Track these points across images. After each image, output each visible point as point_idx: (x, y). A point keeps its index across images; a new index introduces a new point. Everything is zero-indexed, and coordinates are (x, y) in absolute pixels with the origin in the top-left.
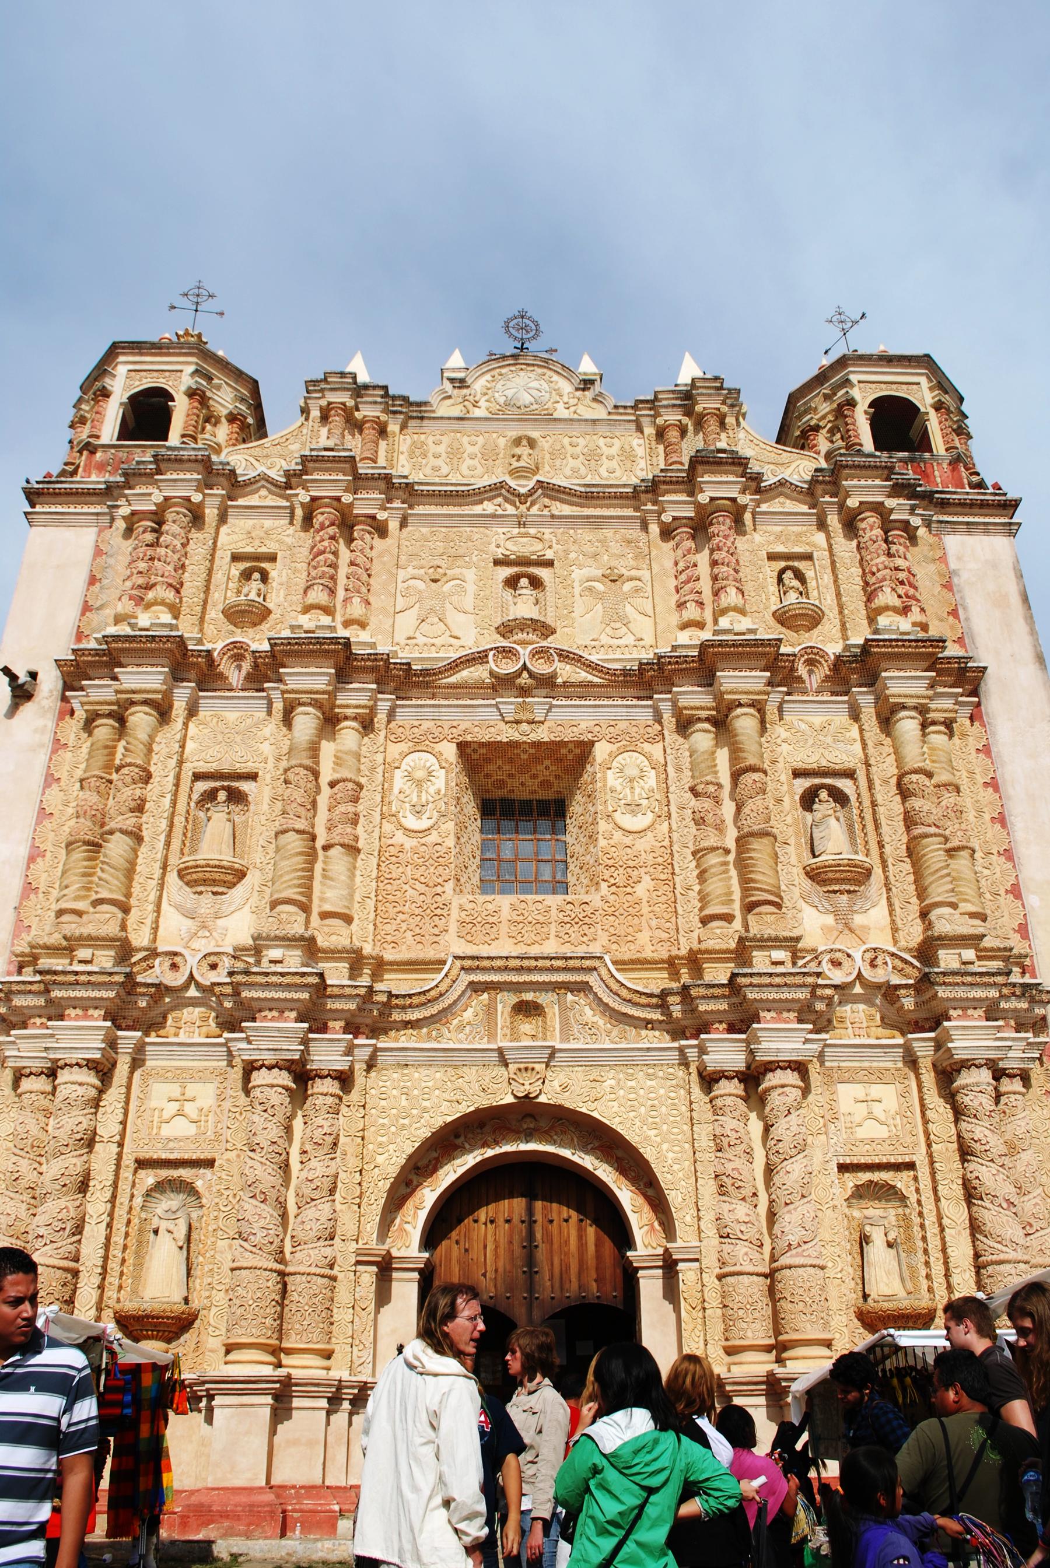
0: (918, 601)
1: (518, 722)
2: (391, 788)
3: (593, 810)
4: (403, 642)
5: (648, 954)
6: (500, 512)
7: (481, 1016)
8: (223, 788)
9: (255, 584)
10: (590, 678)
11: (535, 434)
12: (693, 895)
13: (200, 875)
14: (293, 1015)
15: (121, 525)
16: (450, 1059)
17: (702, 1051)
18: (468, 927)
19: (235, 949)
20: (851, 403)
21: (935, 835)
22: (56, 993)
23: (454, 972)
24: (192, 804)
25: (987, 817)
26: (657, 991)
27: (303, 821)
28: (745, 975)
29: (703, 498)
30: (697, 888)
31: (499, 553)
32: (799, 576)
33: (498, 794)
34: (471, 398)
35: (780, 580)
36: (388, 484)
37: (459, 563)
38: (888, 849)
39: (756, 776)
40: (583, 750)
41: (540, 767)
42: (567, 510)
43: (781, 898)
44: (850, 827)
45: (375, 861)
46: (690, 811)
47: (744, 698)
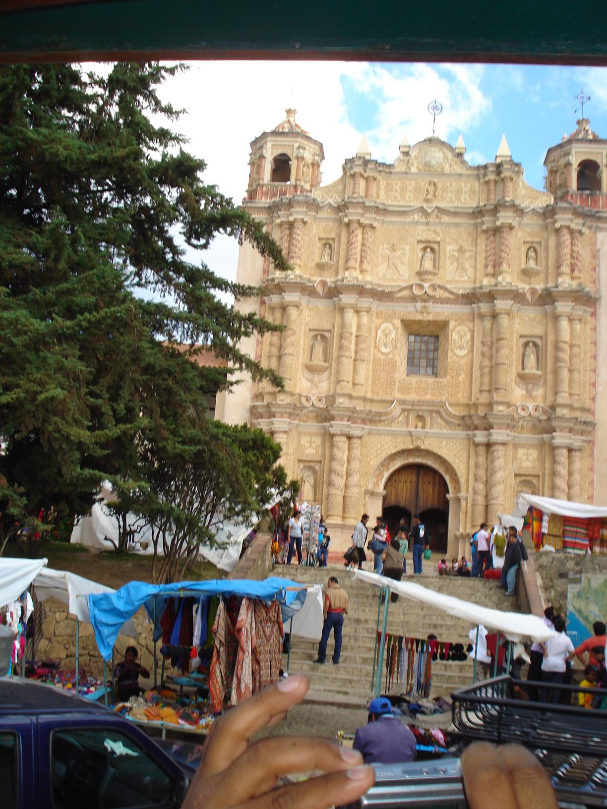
5: (461, 401)
11: (436, 180)
16: (394, 434)
17: (475, 435)
20: (568, 164)
22: (273, 409)
25: (588, 356)
29: (498, 223)
31: (419, 238)
35: (527, 255)
36: (377, 210)
39: (503, 342)
40: (445, 324)
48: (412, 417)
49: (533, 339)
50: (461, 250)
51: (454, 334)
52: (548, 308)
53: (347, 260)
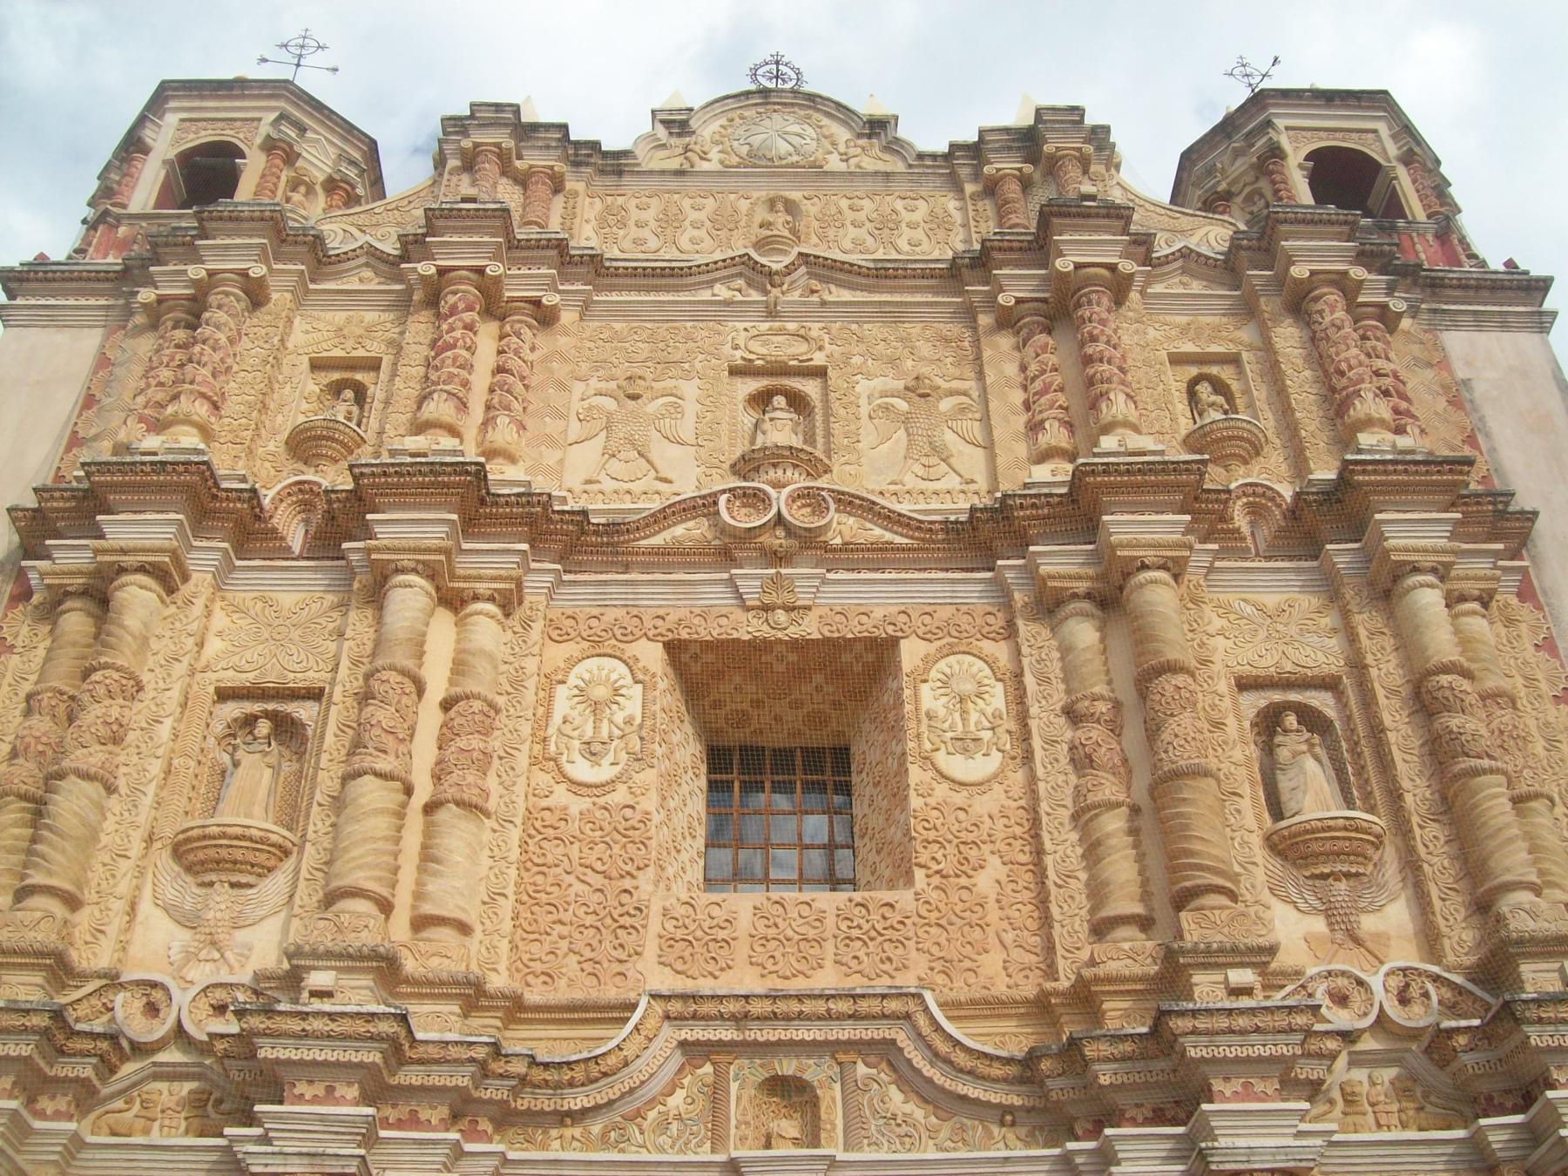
0: (1416, 418)
1: (767, 608)
2: (548, 714)
3: (898, 750)
4: (578, 488)
5: (1001, 989)
6: (739, 297)
7: (700, 1104)
8: (267, 715)
9: (342, 410)
10: (888, 536)
11: (796, 195)
12: (1078, 886)
13: (212, 853)
14: (353, 1092)
15: (139, 319)
18: (681, 944)
19: (257, 976)
21: (1492, 771)
23: (652, 1023)
24: (212, 741)
26: (1019, 1055)
27: (391, 758)
28: (1182, 1014)
29: (1064, 264)
30: (1083, 876)
32: (1219, 387)
33: (734, 737)
34: (697, 148)
36: (561, 253)
37: (673, 372)
38: (1408, 798)
39: (1180, 680)
40: (877, 657)
41: (807, 688)
42: (847, 295)
43: (1235, 878)
44: (1340, 773)
45: (515, 834)
46: (1065, 747)
47: (1149, 555)
48: (743, 1080)
49: (1294, 696)
50: (919, 391)
51: (925, 689)
52: (1341, 554)
53: (422, 400)
